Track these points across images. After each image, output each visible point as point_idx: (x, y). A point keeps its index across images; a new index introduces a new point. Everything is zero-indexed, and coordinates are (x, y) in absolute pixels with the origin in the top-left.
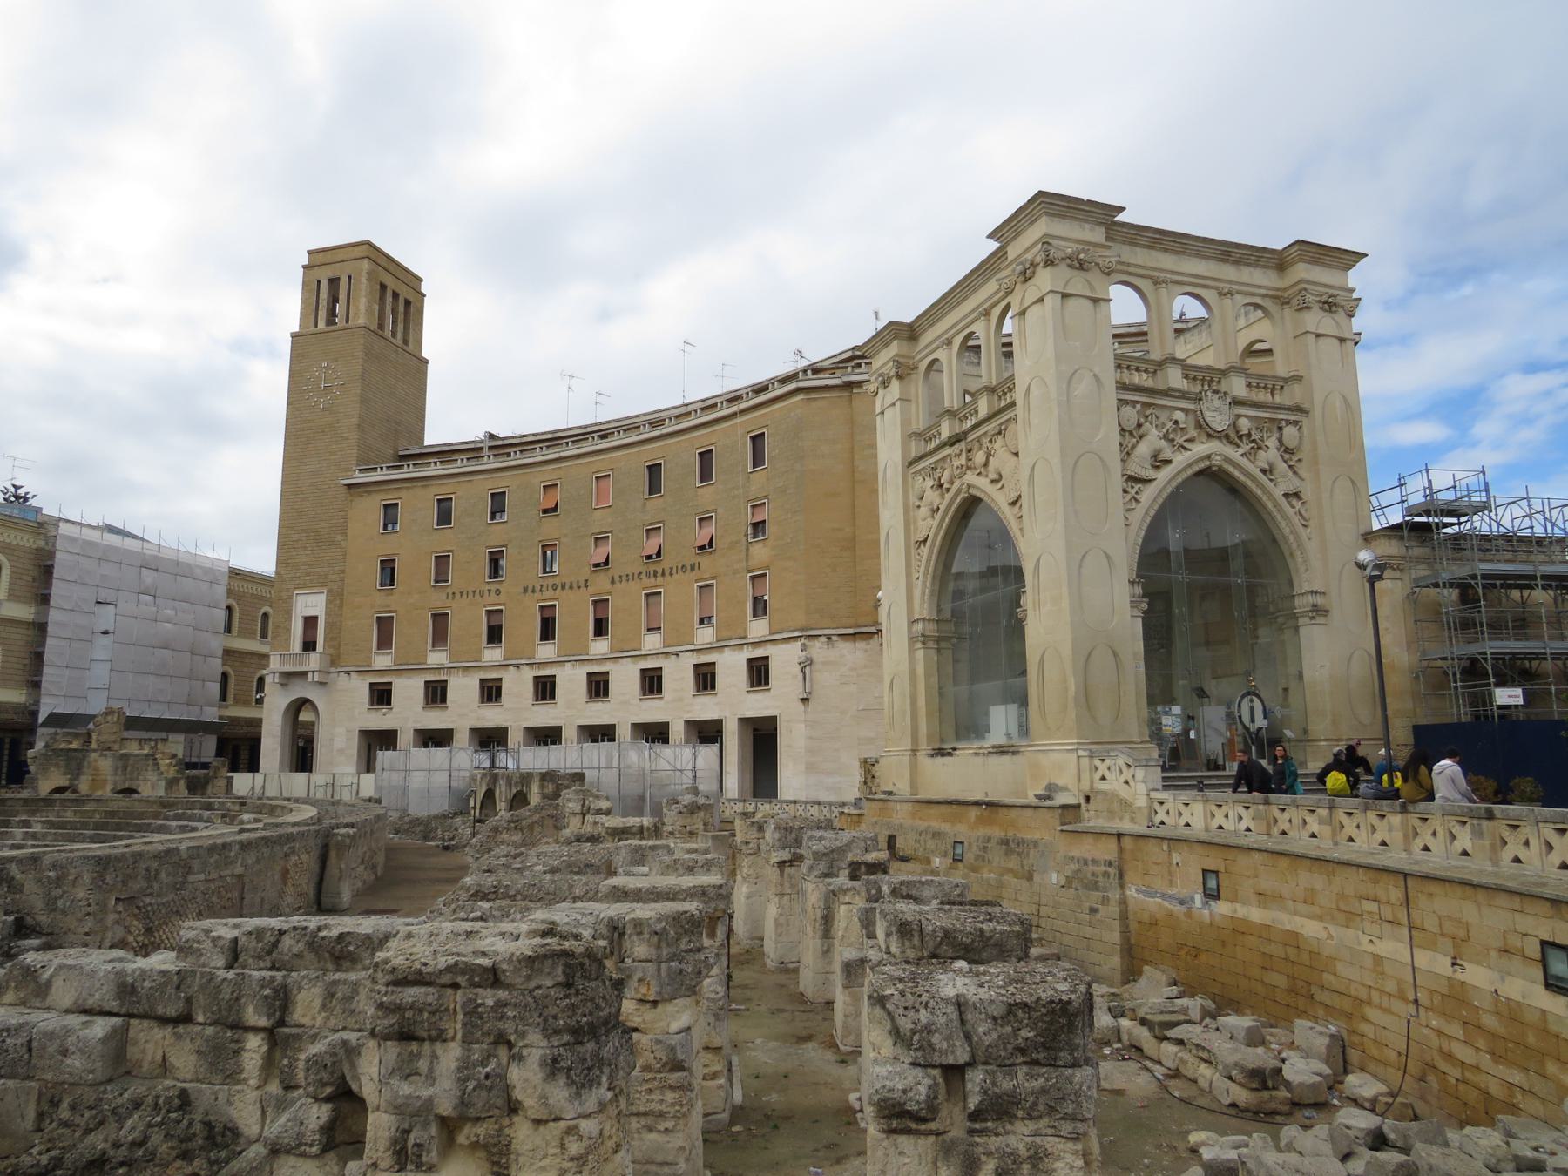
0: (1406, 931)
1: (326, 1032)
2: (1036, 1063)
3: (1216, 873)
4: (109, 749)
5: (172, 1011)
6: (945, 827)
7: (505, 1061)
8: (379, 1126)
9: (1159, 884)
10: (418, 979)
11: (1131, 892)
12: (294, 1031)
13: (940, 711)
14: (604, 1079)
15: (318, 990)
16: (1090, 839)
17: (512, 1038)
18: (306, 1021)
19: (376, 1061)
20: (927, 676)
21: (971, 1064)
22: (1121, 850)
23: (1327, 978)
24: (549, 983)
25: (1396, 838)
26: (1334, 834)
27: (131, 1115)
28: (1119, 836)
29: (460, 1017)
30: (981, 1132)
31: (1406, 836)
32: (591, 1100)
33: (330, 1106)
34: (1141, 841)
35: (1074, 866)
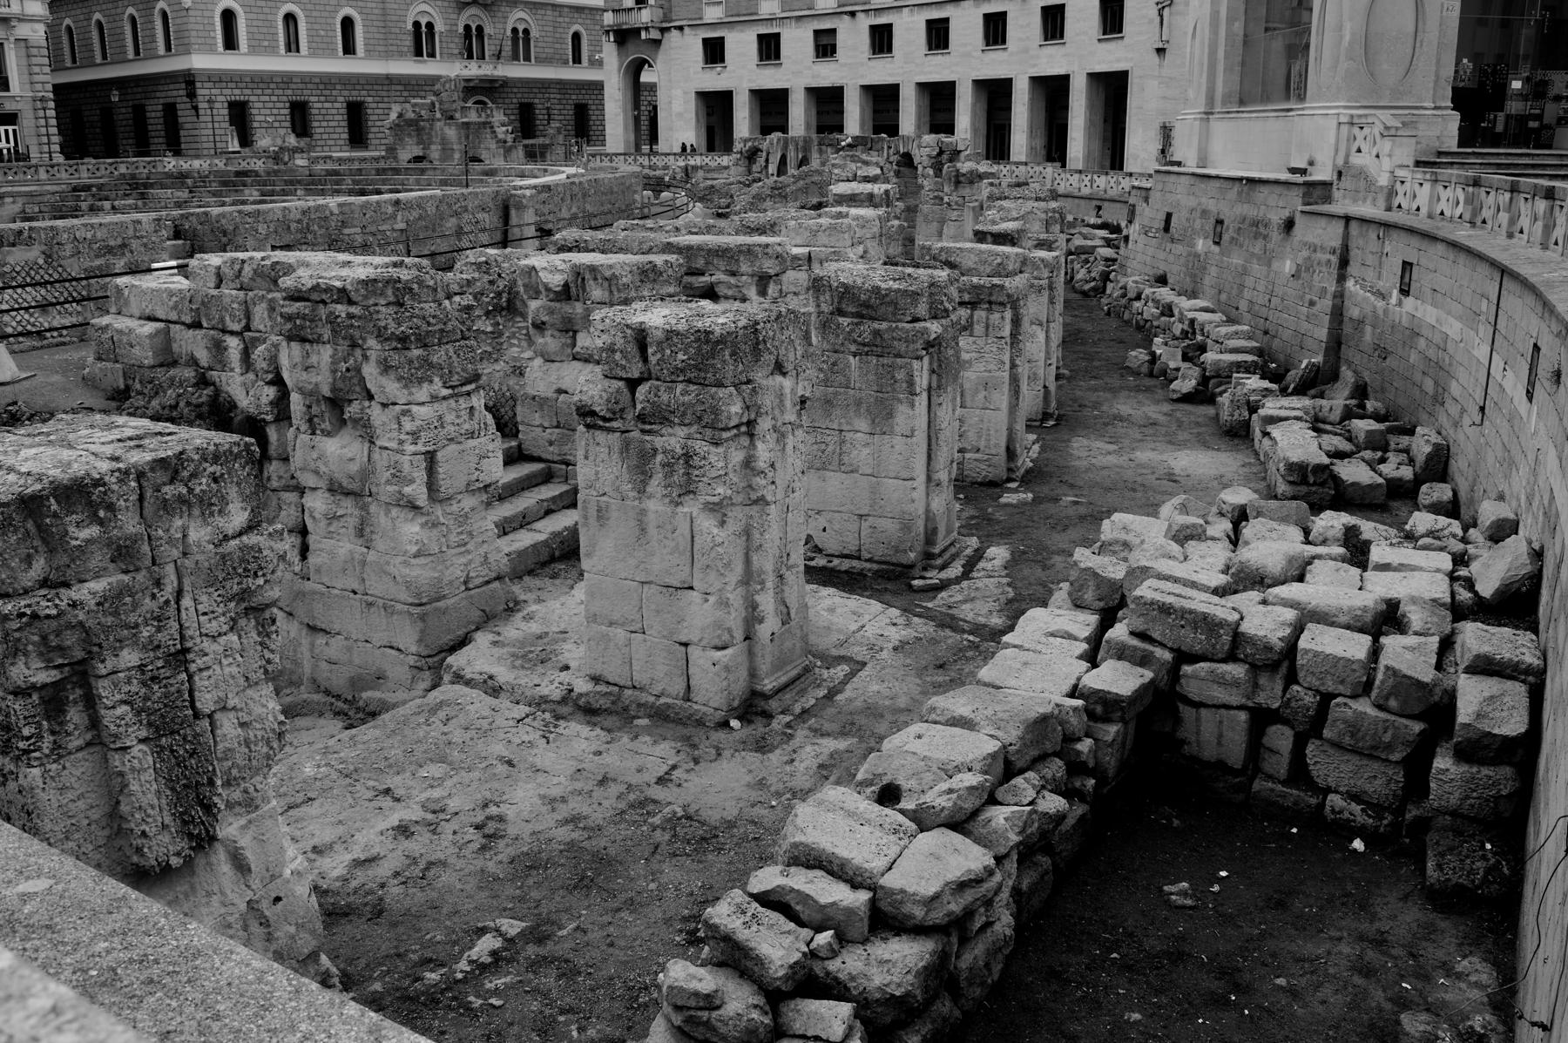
2: (689, 381)
4: (451, 118)
5: (188, 320)
13: (1243, 64)
14: (436, 379)
15: (264, 305)
18: (261, 327)
20: (1230, 20)
30: (649, 432)
32: (422, 393)
35: (1305, 253)
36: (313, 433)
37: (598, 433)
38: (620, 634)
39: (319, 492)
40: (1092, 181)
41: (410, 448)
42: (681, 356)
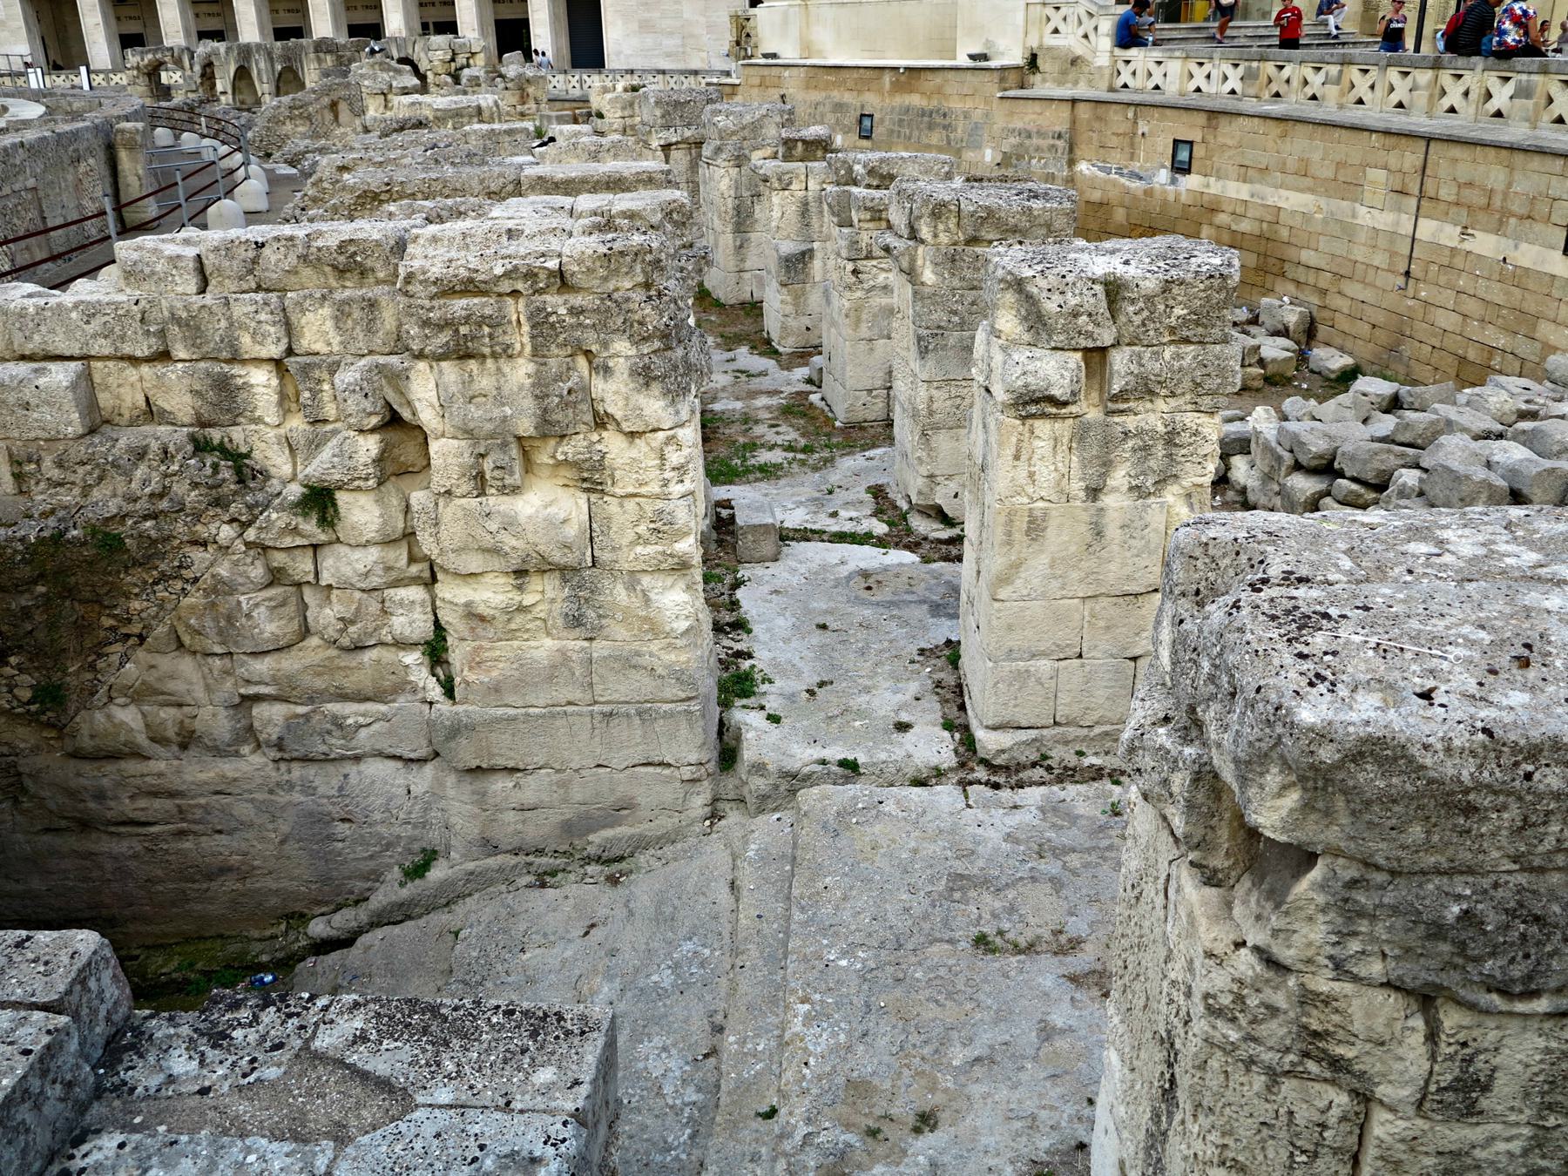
0: (1413, 202)
1: (350, 359)
2: (1187, 341)
3: (1191, 143)
5: (142, 350)
6: (848, 97)
7: (586, 373)
8: (446, 453)
9: (1116, 158)
10: (470, 287)
11: (1083, 167)
12: (308, 359)
15: (326, 311)
16: (1037, 106)
17: (594, 348)
18: (319, 347)
19: (432, 385)
21: (1117, 344)
22: (1074, 122)
23: (1307, 256)
24: (628, 285)
25: (1421, 98)
26: (1342, 94)
27: (136, 466)
28: (1074, 101)
29: (526, 328)
31: (1431, 96)
33: (377, 437)
34: (1102, 109)
35: (1014, 140)
36: (482, 493)
37: (1038, 423)
38: (1044, 666)
39: (488, 578)
40: (581, 81)
41: (676, 489)
42: (1179, 311)
